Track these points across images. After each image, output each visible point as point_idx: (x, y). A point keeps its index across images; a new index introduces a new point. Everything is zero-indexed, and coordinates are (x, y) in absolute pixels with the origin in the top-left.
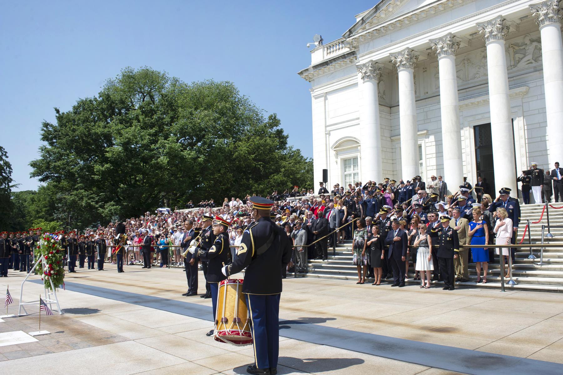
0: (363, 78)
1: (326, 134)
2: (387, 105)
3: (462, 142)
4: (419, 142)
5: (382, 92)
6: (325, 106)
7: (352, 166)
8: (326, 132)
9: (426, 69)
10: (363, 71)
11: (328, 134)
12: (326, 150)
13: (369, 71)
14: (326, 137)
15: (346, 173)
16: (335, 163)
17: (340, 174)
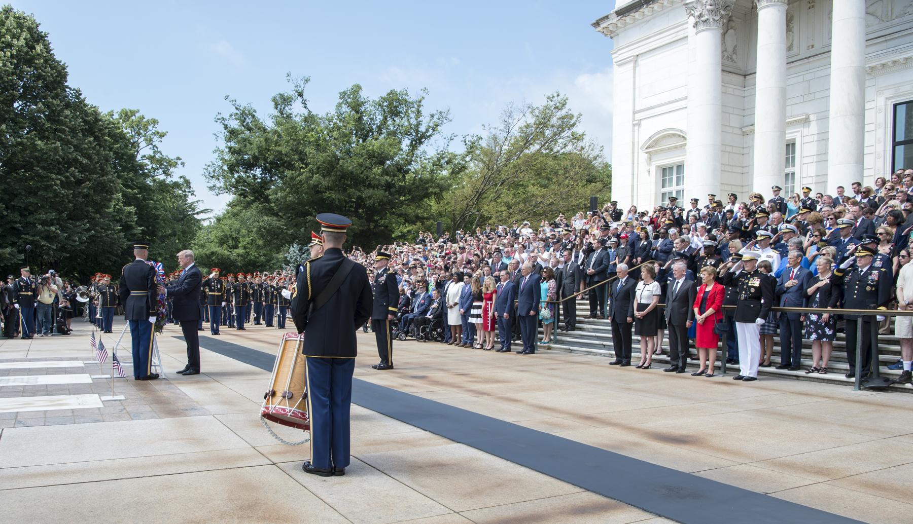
0: (696, 25)
1: (634, 125)
2: (739, 72)
3: (865, 133)
4: (787, 136)
5: (730, 49)
6: (634, 77)
7: (674, 177)
8: (634, 122)
9: (813, 4)
10: (697, 13)
11: (637, 124)
12: (633, 153)
13: (707, 12)
14: (634, 131)
15: (664, 190)
16: (647, 173)
17: (653, 191)
